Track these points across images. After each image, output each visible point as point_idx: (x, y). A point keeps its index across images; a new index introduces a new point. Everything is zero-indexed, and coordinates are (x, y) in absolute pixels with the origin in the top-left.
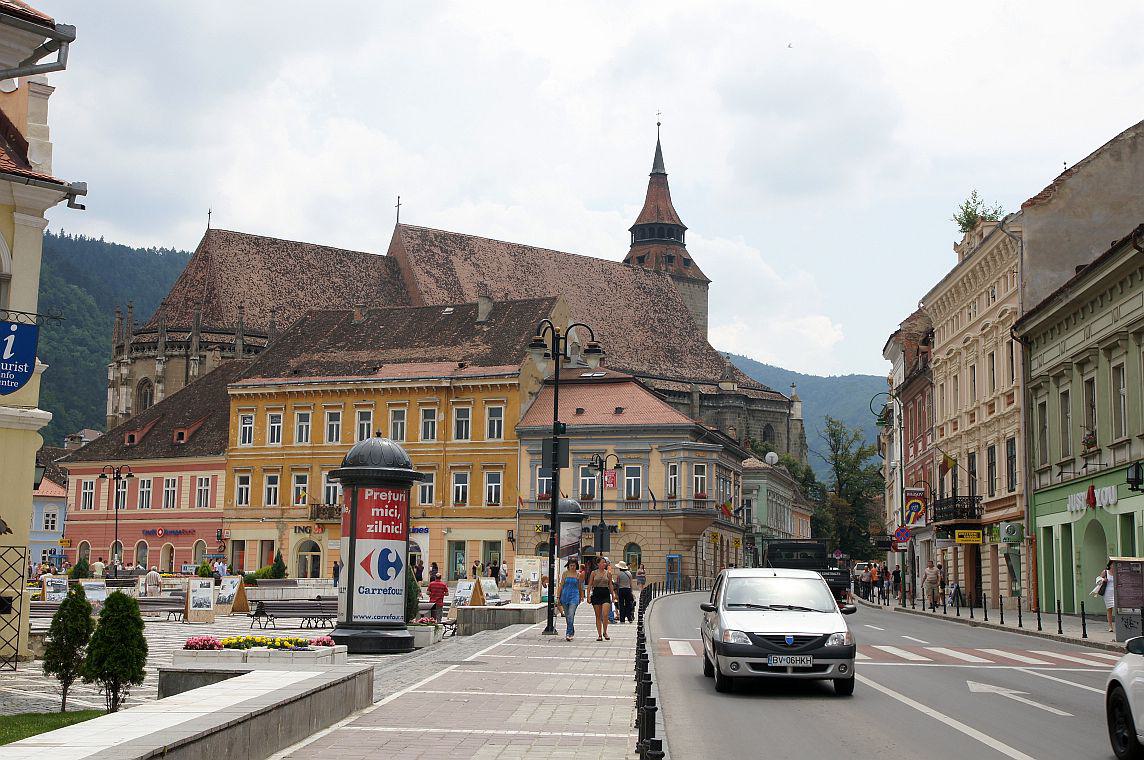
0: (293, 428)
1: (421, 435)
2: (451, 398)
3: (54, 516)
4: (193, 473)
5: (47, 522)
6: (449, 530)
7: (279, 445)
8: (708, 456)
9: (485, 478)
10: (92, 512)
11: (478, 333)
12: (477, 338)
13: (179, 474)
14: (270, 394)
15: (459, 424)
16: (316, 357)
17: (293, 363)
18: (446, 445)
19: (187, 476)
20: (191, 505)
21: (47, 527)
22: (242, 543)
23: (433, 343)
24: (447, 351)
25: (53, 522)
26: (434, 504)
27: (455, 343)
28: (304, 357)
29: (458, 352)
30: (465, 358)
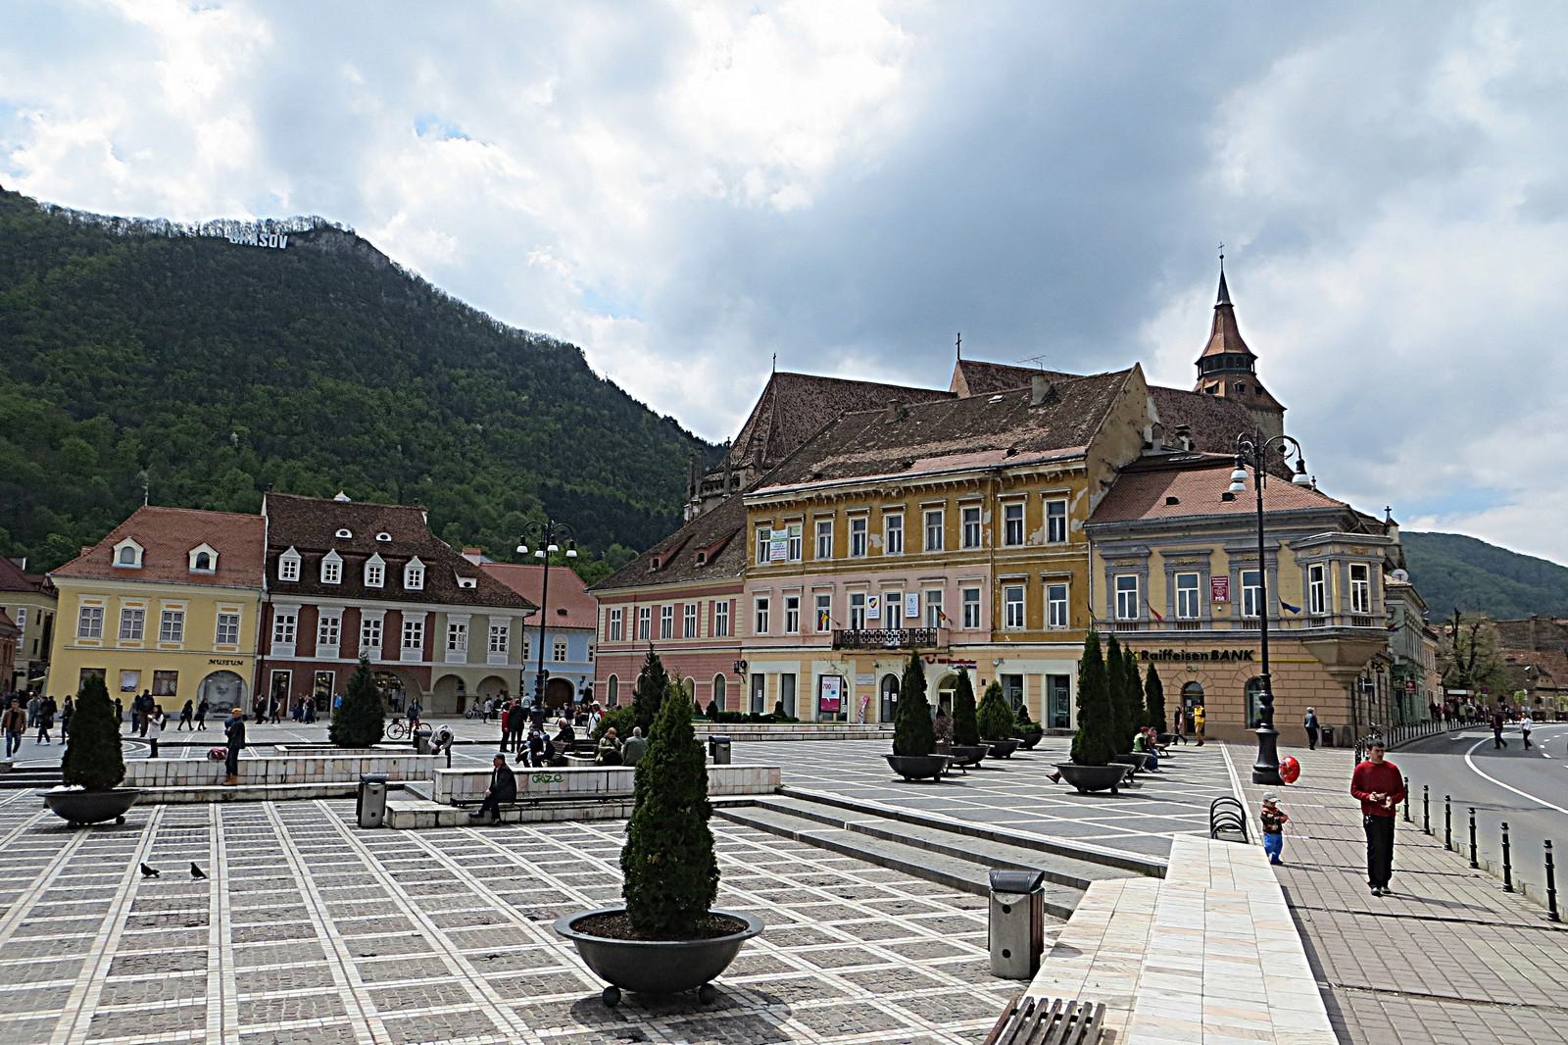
0: (813, 542)
1: (962, 542)
2: (998, 492)
3: (563, 647)
4: (712, 598)
5: (557, 653)
6: (1001, 660)
7: (799, 561)
8: (1371, 551)
9: (1046, 593)
10: (620, 643)
11: (1032, 417)
12: (1031, 424)
13: (624, 605)
14: (788, 502)
15: (1010, 525)
16: (841, 459)
17: (816, 468)
18: (994, 552)
19: (705, 600)
20: (710, 635)
21: (557, 658)
22: (762, 676)
23: (976, 433)
24: (993, 440)
25: (563, 653)
26: (980, 628)
27: (1004, 430)
28: (830, 460)
29: (1008, 439)
30: (1016, 444)
